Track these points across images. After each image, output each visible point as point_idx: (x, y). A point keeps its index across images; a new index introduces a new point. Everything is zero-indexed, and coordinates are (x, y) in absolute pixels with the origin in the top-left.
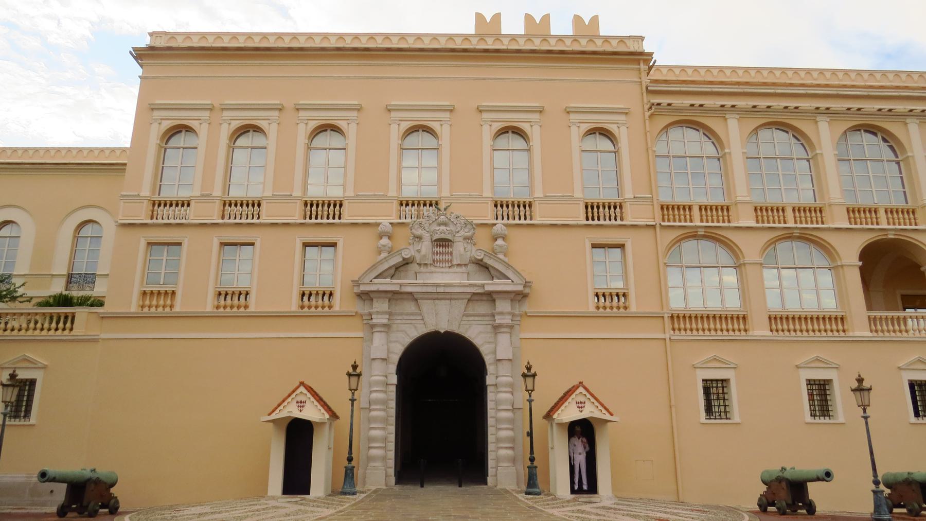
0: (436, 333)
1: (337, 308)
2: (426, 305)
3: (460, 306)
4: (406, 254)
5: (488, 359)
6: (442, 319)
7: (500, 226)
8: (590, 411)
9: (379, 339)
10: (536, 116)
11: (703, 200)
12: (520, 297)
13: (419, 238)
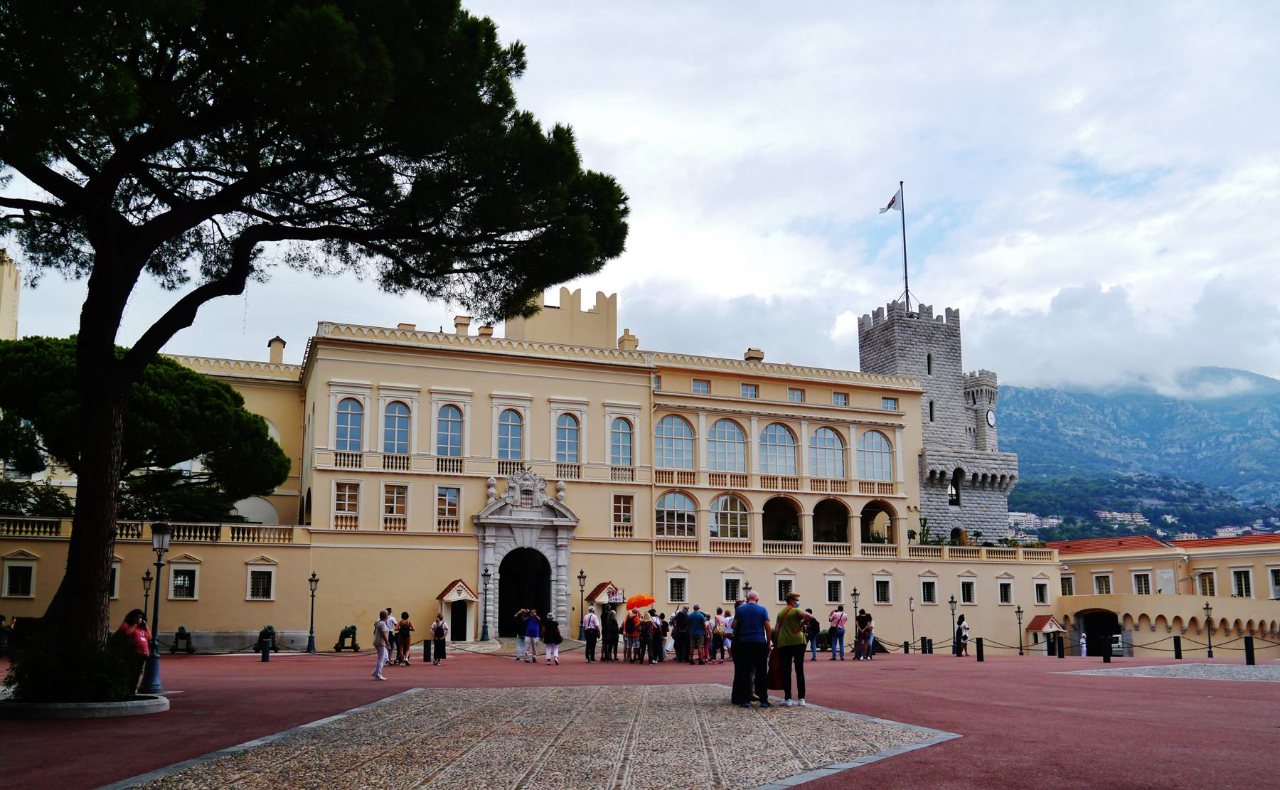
0: (522, 549)
1: (462, 531)
2: (517, 532)
3: (536, 533)
5: (552, 565)
6: (527, 540)
9: (490, 551)
10: (583, 408)
11: (680, 469)
13: (513, 488)
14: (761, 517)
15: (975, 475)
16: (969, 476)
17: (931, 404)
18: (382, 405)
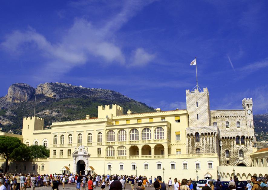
4: (76, 151)
5: (85, 163)
7: (87, 147)
8: (90, 169)
12: (89, 156)
14: (129, 151)
15: (202, 134)
16: (200, 134)
17: (198, 115)
18: (60, 136)
